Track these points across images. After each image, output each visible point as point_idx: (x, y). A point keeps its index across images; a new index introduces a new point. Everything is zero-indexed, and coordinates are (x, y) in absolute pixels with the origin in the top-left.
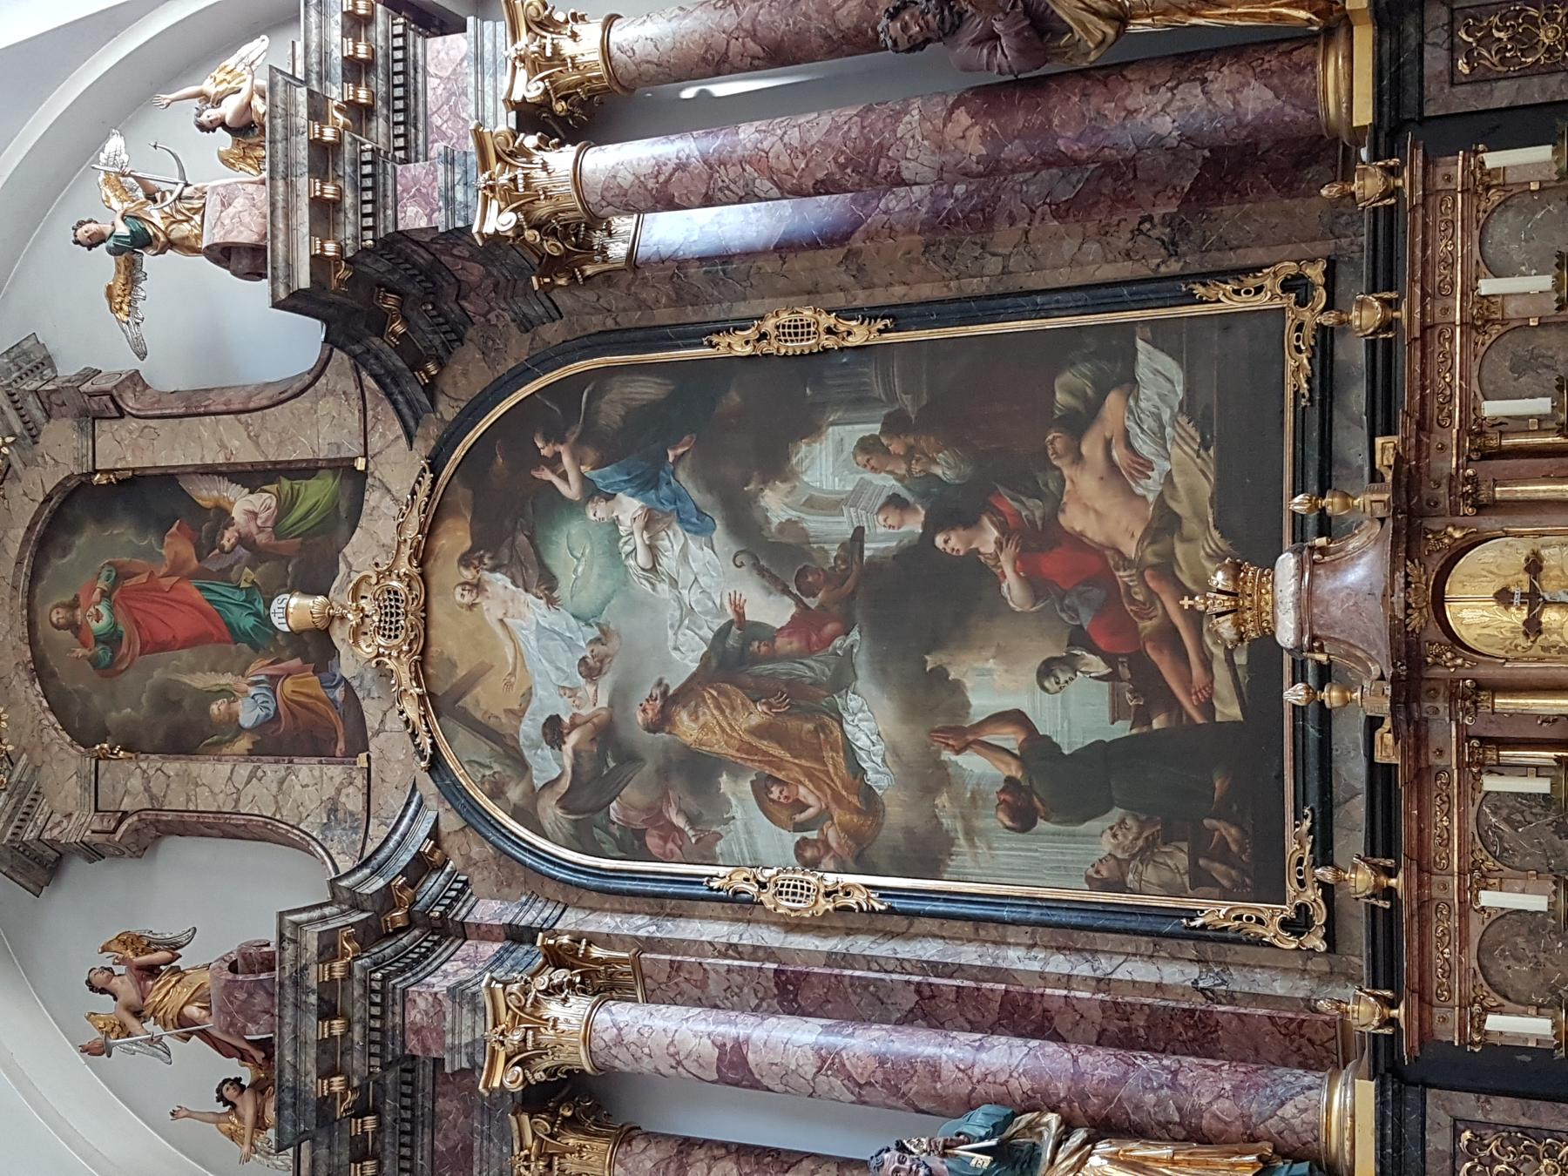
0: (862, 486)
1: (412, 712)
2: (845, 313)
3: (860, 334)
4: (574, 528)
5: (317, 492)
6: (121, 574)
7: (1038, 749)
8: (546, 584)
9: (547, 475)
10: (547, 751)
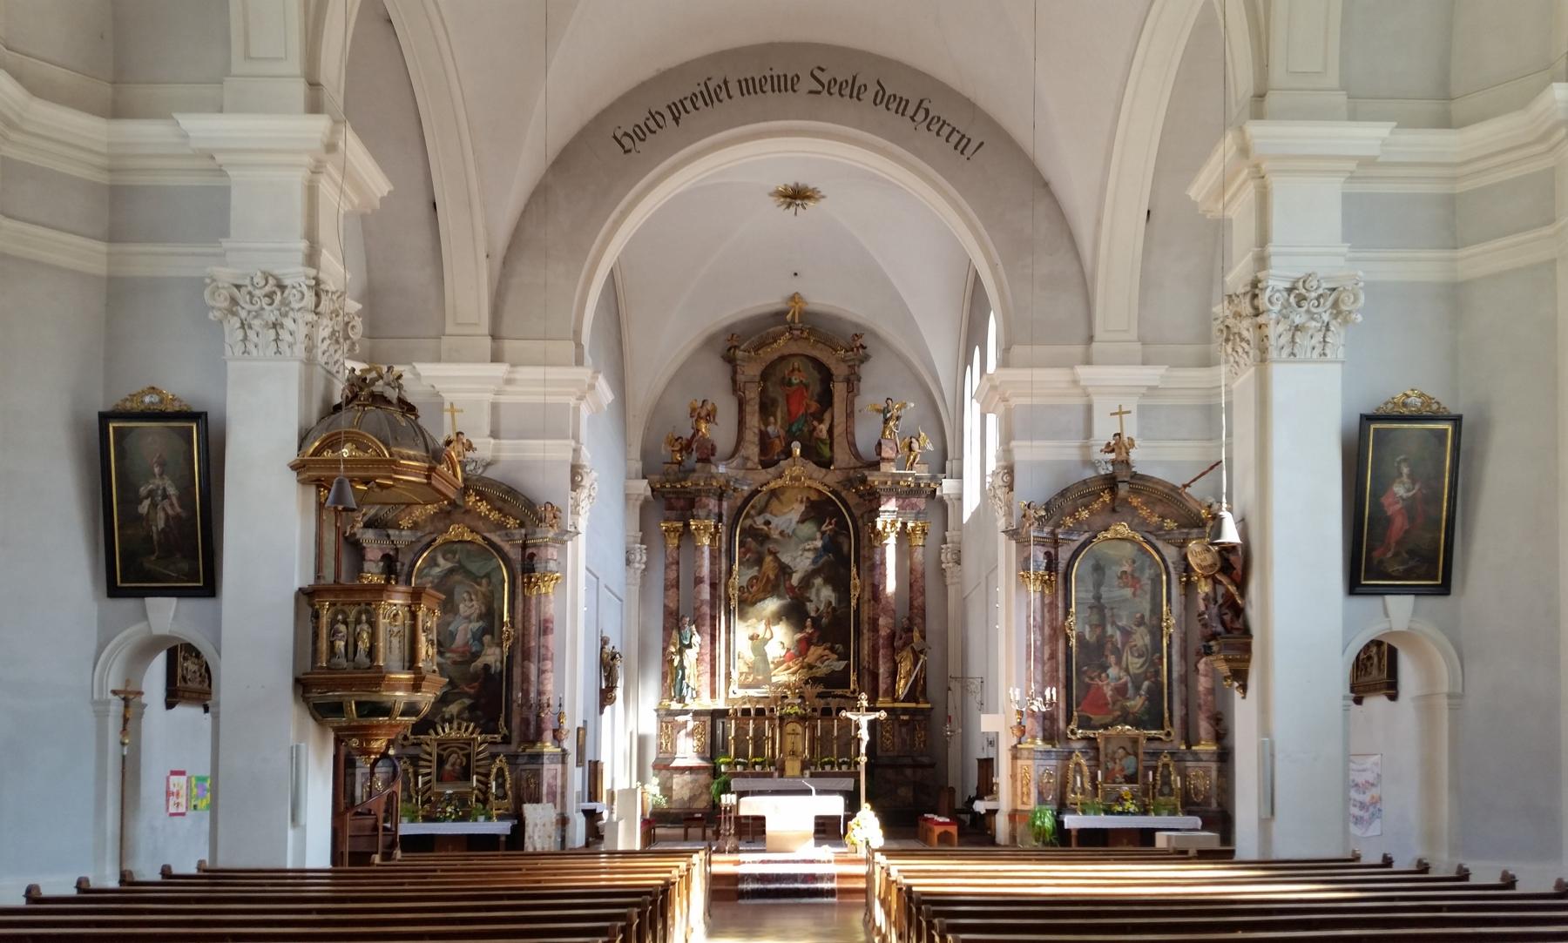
0: (821, 602)
1: (772, 485)
2: (858, 599)
3: (853, 603)
4: (815, 529)
5: (826, 451)
6: (806, 386)
7: (765, 641)
8: (802, 521)
9: (827, 521)
10: (763, 521)
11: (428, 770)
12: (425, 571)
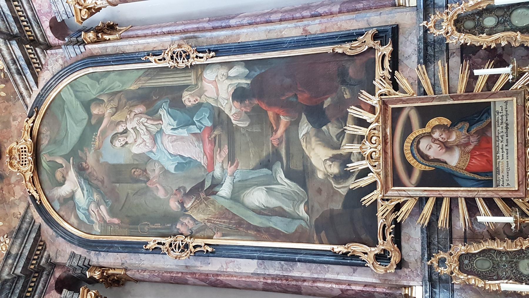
11: (462, 206)
12: (82, 216)
